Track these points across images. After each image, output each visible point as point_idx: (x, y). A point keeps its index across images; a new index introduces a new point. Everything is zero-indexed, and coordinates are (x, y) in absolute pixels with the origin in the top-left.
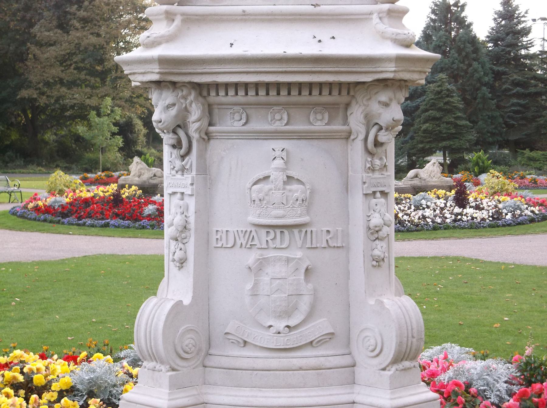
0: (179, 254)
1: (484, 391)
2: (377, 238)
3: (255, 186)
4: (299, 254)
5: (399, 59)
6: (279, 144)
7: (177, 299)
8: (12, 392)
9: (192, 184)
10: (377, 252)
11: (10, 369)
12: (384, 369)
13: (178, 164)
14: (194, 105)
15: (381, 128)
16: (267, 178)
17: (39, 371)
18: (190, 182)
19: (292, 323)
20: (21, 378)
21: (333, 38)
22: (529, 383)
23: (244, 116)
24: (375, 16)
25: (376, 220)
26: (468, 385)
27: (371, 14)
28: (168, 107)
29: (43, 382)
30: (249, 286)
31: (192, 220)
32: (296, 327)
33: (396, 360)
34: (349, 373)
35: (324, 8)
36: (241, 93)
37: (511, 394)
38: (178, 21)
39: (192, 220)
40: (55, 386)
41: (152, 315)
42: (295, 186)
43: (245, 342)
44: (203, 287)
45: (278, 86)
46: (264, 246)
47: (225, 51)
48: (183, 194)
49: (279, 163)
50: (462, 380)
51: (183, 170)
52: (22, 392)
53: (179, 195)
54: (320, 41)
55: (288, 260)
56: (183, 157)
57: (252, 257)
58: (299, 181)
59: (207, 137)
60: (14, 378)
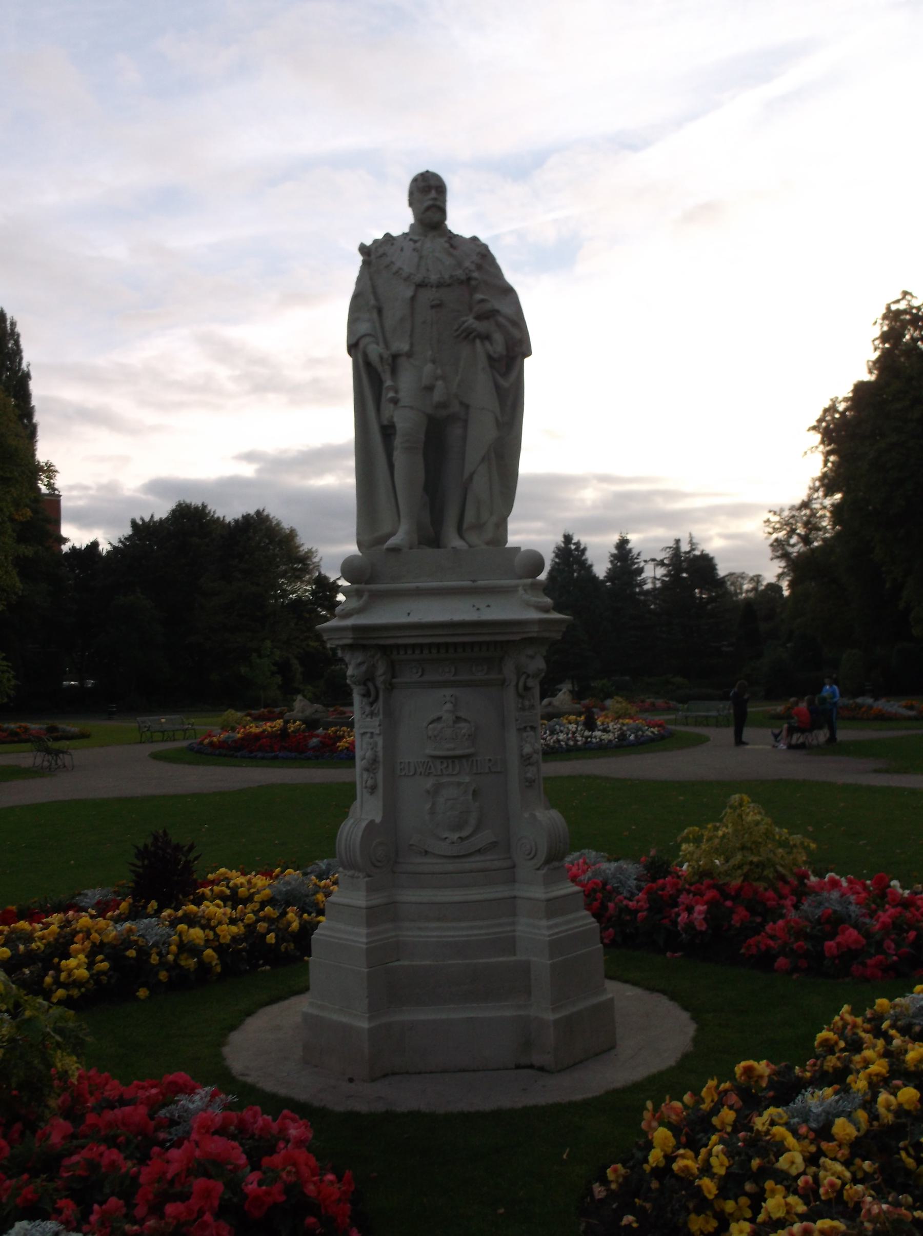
0: (370, 782)
1: (618, 887)
2: (529, 764)
3: (431, 726)
4: (467, 779)
5: (541, 622)
6: (448, 692)
7: (370, 818)
8: (221, 903)
9: (380, 725)
10: (529, 775)
11: (218, 884)
12: (538, 869)
13: (368, 709)
14: (380, 663)
15: (528, 676)
16: (439, 719)
17: (242, 885)
18: (377, 723)
19: (464, 834)
20: (228, 892)
21: (488, 606)
22: (654, 880)
23: (420, 670)
24: (520, 588)
25: (527, 749)
26: (605, 884)
27: (517, 586)
28: (359, 665)
29: (247, 894)
30: (428, 806)
31: (380, 754)
32: (467, 838)
33: (548, 861)
34: (510, 875)
35: (480, 583)
36: (418, 652)
37: (640, 889)
38: (365, 597)
39: (380, 754)
40: (257, 898)
41: (351, 831)
42: (462, 725)
43: (426, 852)
44: (391, 809)
45: (447, 645)
46: (439, 773)
47: (403, 619)
48: (372, 733)
49: (449, 706)
50: (599, 879)
51: (372, 714)
52: (230, 903)
53: (369, 735)
54: (478, 609)
55: (459, 784)
56: (372, 704)
57: (429, 783)
58: (465, 720)
59: (391, 687)
60: (222, 891)
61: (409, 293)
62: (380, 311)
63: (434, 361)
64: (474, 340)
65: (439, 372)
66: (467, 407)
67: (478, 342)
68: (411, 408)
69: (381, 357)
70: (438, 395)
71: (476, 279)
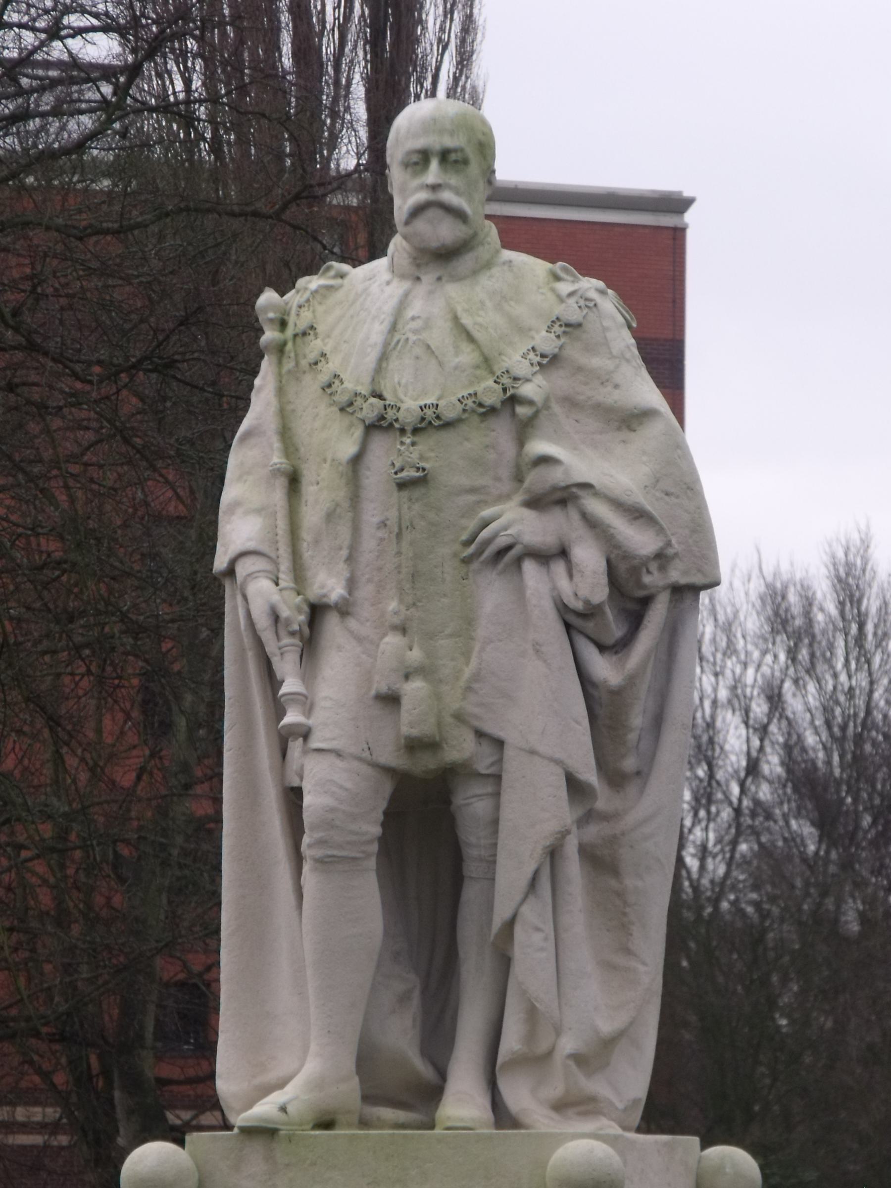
61: (348, 448)
62: (294, 481)
63: (403, 629)
64: (518, 562)
65: (415, 656)
66: (499, 744)
67: (530, 567)
68: (338, 753)
69: (276, 618)
70: (413, 718)
71: (530, 403)
